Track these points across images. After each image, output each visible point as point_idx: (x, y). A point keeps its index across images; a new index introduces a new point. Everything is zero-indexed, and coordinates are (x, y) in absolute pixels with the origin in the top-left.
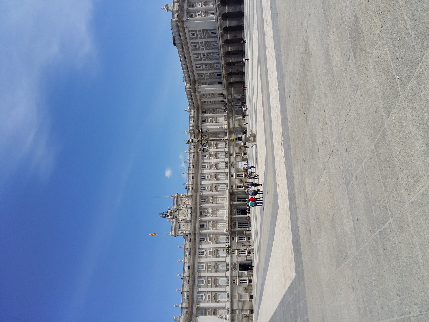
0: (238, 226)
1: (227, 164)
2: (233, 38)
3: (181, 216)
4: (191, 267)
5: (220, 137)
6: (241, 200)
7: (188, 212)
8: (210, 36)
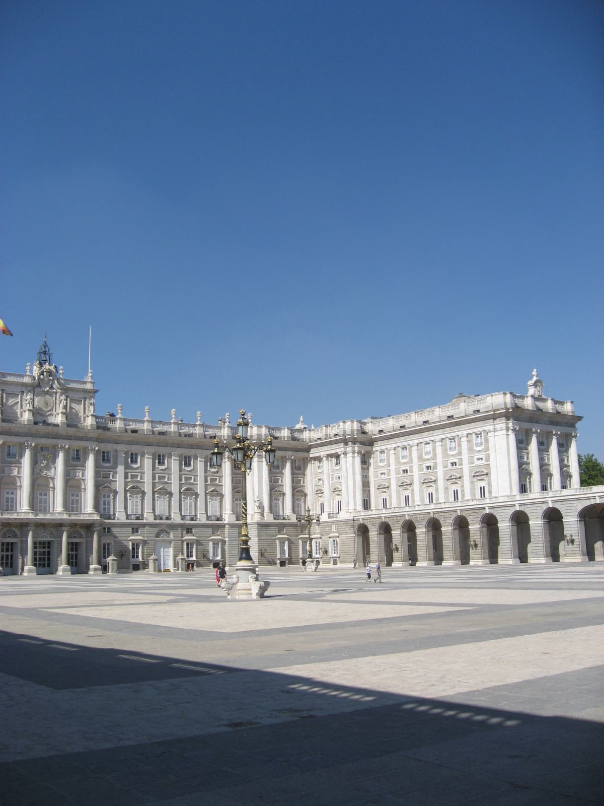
0: (8, 544)
1: (167, 519)
2: (471, 538)
6: (72, 553)
8: (476, 483)
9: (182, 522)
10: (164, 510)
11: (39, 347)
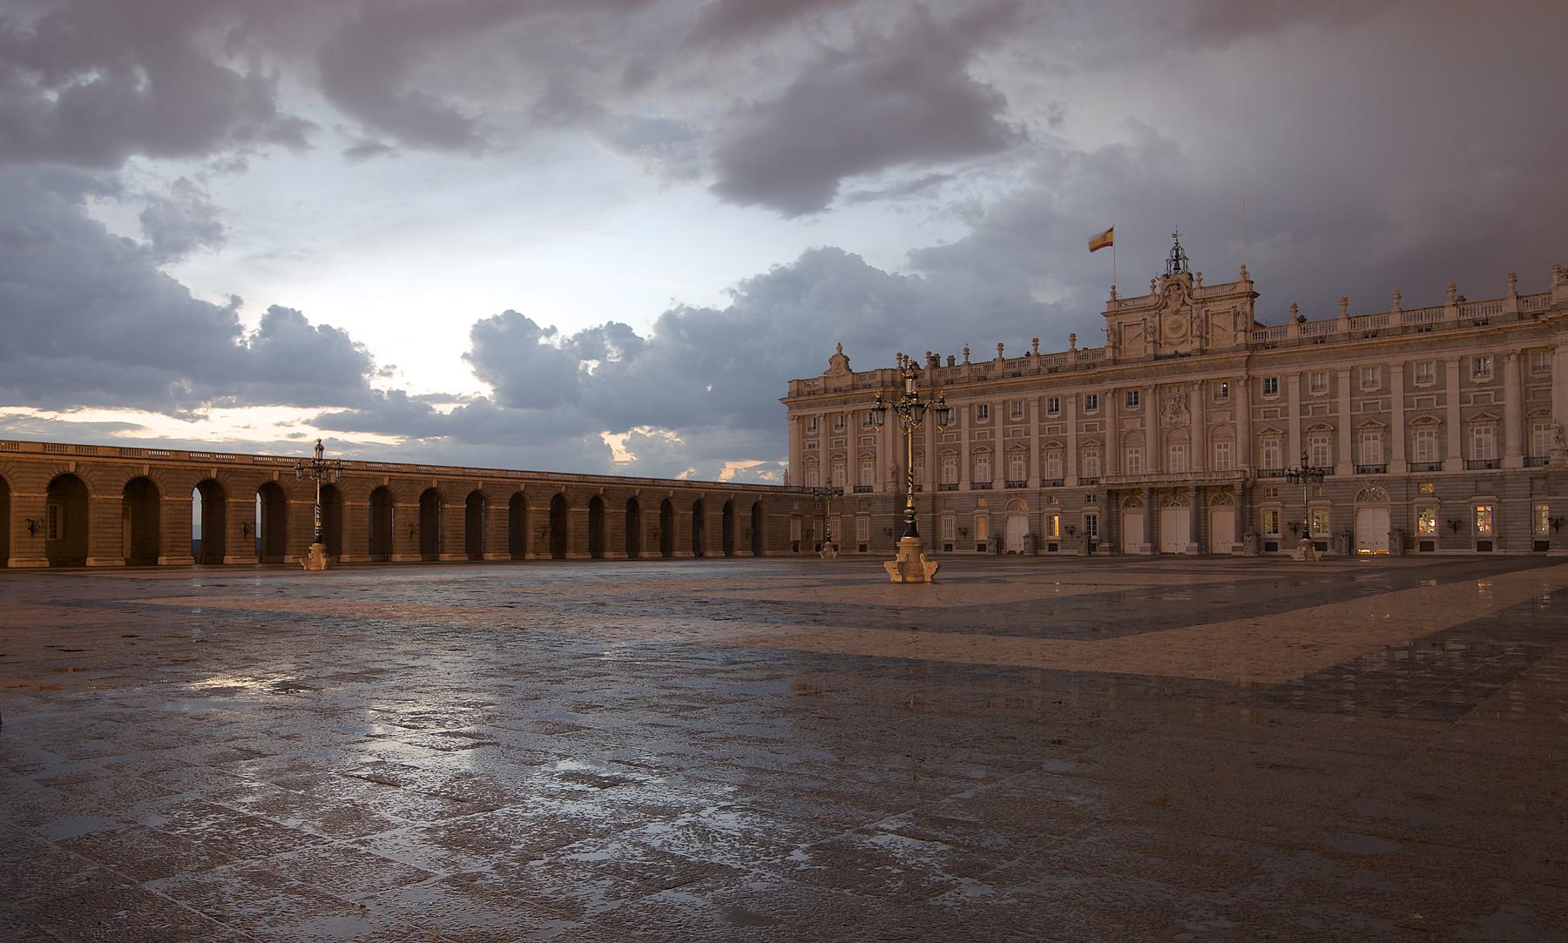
1: (1377, 471)
3: (1168, 320)
4: (1018, 379)
5: (1535, 433)
7: (1182, 343)
9: (1407, 474)
10: (1376, 458)
11: (1166, 254)
